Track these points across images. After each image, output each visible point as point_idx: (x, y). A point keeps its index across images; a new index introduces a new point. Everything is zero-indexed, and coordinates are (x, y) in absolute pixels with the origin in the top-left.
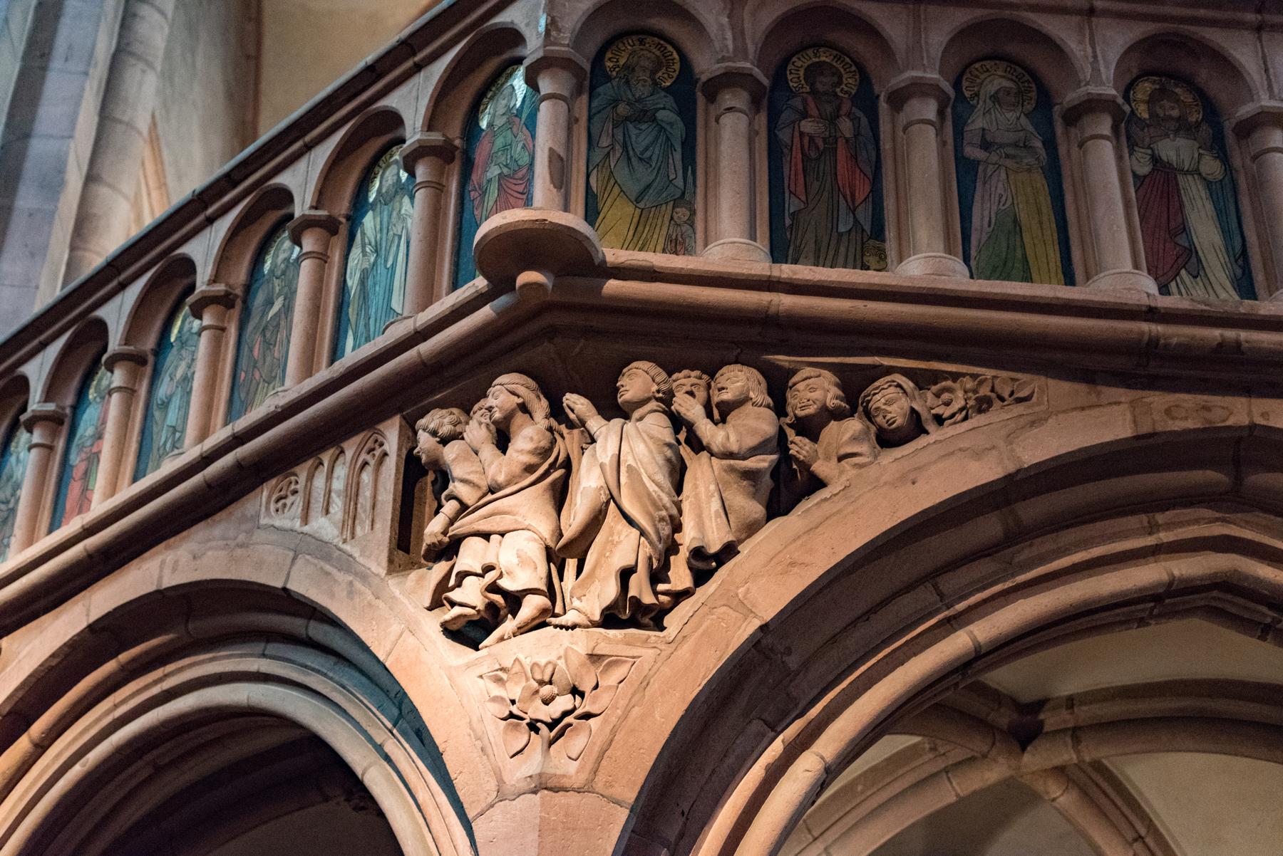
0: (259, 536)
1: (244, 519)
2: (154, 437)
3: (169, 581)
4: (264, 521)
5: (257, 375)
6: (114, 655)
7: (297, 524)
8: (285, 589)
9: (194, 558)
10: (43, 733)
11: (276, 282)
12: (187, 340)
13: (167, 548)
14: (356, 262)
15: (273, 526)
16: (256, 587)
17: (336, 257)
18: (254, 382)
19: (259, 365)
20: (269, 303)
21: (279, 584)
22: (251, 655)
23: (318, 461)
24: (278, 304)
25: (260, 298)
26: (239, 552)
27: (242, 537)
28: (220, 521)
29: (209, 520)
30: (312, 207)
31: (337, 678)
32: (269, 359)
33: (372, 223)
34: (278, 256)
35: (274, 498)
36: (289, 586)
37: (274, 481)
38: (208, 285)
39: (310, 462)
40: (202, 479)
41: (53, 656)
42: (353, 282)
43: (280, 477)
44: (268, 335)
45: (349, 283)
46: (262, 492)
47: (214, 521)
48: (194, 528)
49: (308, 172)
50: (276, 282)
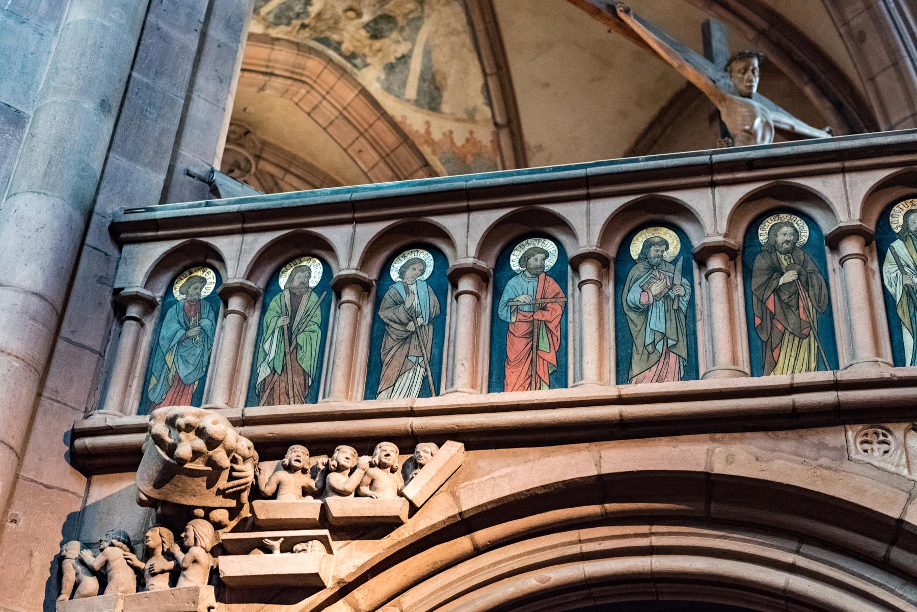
0: (846, 465)
1: (822, 446)
2: (634, 334)
3: (719, 468)
4: (853, 455)
5: (780, 327)
6: (601, 502)
7: (905, 472)
8: (900, 522)
9: (757, 459)
10: (489, 542)
11: (782, 257)
12: (658, 265)
13: (714, 440)
14: (894, 275)
15: (870, 463)
16: (849, 507)
17: (875, 265)
18: (775, 330)
19: (780, 316)
20: (777, 271)
21: (895, 514)
22: (779, 548)
23: (911, 427)
24: (789, 277)
25: (761, 263)
26: (826, 473)
27: (823, 461)
28: (786, 438)
29: (770, 433)
30: (860, 220)
31: (909, 597)
32: (792, 318)
33: (905, 250)
34: (776, 235)
35: (859, 440)
36: (907, 519)
37: (860, 427)
38: (724, 237)
39: (905, 425)
40: (791, 403)
41: (543, 487)
42: (897, 292)
43: (867, 426)
44: (785, 297)
45: (891, 290)
46: (846, 432)
47: (778, 436)
48: (748, 434)
49: (846, 190)
50: (782, 257)
